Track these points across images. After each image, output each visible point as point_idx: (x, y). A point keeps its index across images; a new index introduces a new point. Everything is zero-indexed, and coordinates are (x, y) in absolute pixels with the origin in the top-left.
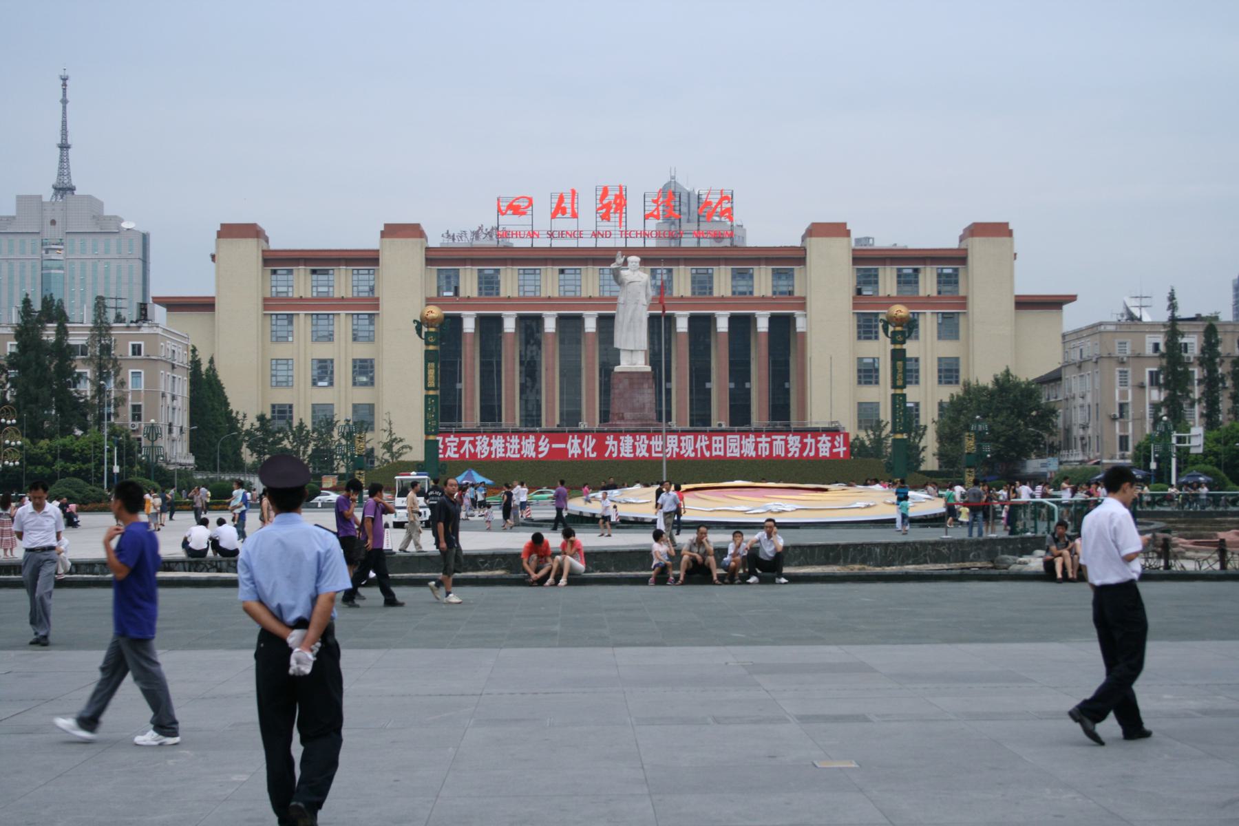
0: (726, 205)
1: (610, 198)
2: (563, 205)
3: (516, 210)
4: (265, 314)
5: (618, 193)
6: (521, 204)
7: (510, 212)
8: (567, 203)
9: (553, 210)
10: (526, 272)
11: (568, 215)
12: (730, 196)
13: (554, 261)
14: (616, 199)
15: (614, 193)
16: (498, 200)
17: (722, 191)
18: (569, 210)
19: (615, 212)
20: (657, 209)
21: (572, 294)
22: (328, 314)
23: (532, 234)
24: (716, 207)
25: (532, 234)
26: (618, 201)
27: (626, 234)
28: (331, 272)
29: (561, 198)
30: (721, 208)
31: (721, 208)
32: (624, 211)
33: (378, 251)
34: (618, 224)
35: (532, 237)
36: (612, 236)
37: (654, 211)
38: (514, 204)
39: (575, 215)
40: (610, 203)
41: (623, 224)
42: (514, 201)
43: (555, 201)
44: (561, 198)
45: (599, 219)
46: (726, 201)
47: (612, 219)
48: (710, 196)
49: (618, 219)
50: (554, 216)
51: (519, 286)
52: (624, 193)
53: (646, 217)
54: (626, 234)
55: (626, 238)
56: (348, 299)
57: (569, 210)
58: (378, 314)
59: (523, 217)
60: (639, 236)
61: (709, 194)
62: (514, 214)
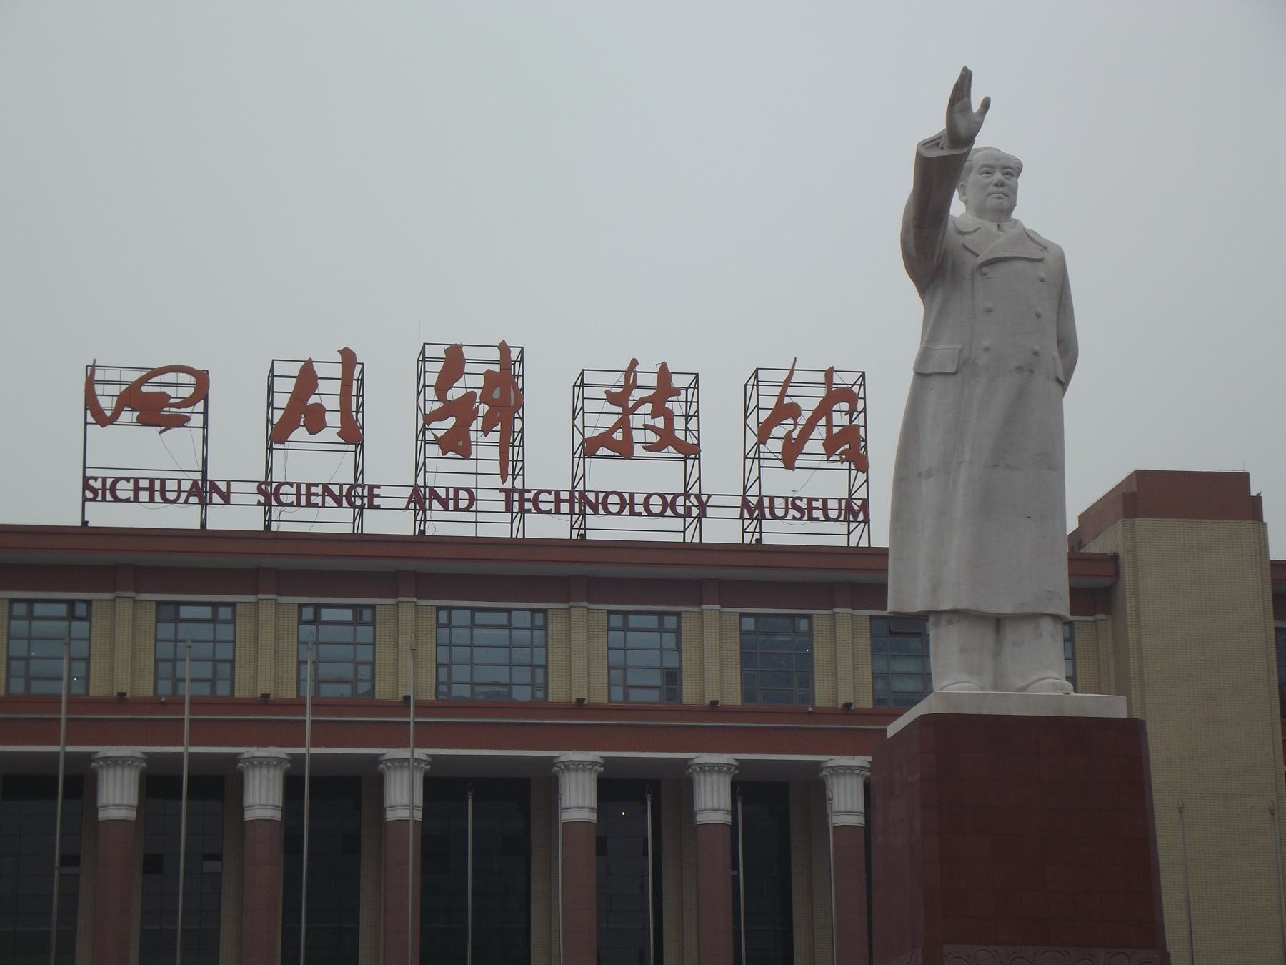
1: (472, 381)
2: (313, 400)
5: (496, 368)
6: (170, 391)
7: (128, 416)
8: (327, 395)
9: (278, 415)
10: (185, 612)
11: (330, 434)
14: (487, 391)
15: (483, 368)
17: (829, 373)
20: (624, 423)
21: (344, 690)
24: (811, 424)
25: (204, 490)
26: (497, 394)
27: (522, 501)
29: (307, 378)
30: (829, 425)
31: (829, 425)
34: (496, 467)
35: (204, 503)
36: (481, 506)
37: (613, 429)
38: (145, 389)
39: (352, 434)
40: (470, 397)
42: (144, 380)
43: (286, 386)
44: (307, 378)
45: (434, 450)
46: (845, 406)
48: (790, 391)
49: (495, 452)
50: (278, 434)
51: (157, 661)
57: (333, 419)
59: (174, 431)
61: (787, 383)
62: (142, 422)
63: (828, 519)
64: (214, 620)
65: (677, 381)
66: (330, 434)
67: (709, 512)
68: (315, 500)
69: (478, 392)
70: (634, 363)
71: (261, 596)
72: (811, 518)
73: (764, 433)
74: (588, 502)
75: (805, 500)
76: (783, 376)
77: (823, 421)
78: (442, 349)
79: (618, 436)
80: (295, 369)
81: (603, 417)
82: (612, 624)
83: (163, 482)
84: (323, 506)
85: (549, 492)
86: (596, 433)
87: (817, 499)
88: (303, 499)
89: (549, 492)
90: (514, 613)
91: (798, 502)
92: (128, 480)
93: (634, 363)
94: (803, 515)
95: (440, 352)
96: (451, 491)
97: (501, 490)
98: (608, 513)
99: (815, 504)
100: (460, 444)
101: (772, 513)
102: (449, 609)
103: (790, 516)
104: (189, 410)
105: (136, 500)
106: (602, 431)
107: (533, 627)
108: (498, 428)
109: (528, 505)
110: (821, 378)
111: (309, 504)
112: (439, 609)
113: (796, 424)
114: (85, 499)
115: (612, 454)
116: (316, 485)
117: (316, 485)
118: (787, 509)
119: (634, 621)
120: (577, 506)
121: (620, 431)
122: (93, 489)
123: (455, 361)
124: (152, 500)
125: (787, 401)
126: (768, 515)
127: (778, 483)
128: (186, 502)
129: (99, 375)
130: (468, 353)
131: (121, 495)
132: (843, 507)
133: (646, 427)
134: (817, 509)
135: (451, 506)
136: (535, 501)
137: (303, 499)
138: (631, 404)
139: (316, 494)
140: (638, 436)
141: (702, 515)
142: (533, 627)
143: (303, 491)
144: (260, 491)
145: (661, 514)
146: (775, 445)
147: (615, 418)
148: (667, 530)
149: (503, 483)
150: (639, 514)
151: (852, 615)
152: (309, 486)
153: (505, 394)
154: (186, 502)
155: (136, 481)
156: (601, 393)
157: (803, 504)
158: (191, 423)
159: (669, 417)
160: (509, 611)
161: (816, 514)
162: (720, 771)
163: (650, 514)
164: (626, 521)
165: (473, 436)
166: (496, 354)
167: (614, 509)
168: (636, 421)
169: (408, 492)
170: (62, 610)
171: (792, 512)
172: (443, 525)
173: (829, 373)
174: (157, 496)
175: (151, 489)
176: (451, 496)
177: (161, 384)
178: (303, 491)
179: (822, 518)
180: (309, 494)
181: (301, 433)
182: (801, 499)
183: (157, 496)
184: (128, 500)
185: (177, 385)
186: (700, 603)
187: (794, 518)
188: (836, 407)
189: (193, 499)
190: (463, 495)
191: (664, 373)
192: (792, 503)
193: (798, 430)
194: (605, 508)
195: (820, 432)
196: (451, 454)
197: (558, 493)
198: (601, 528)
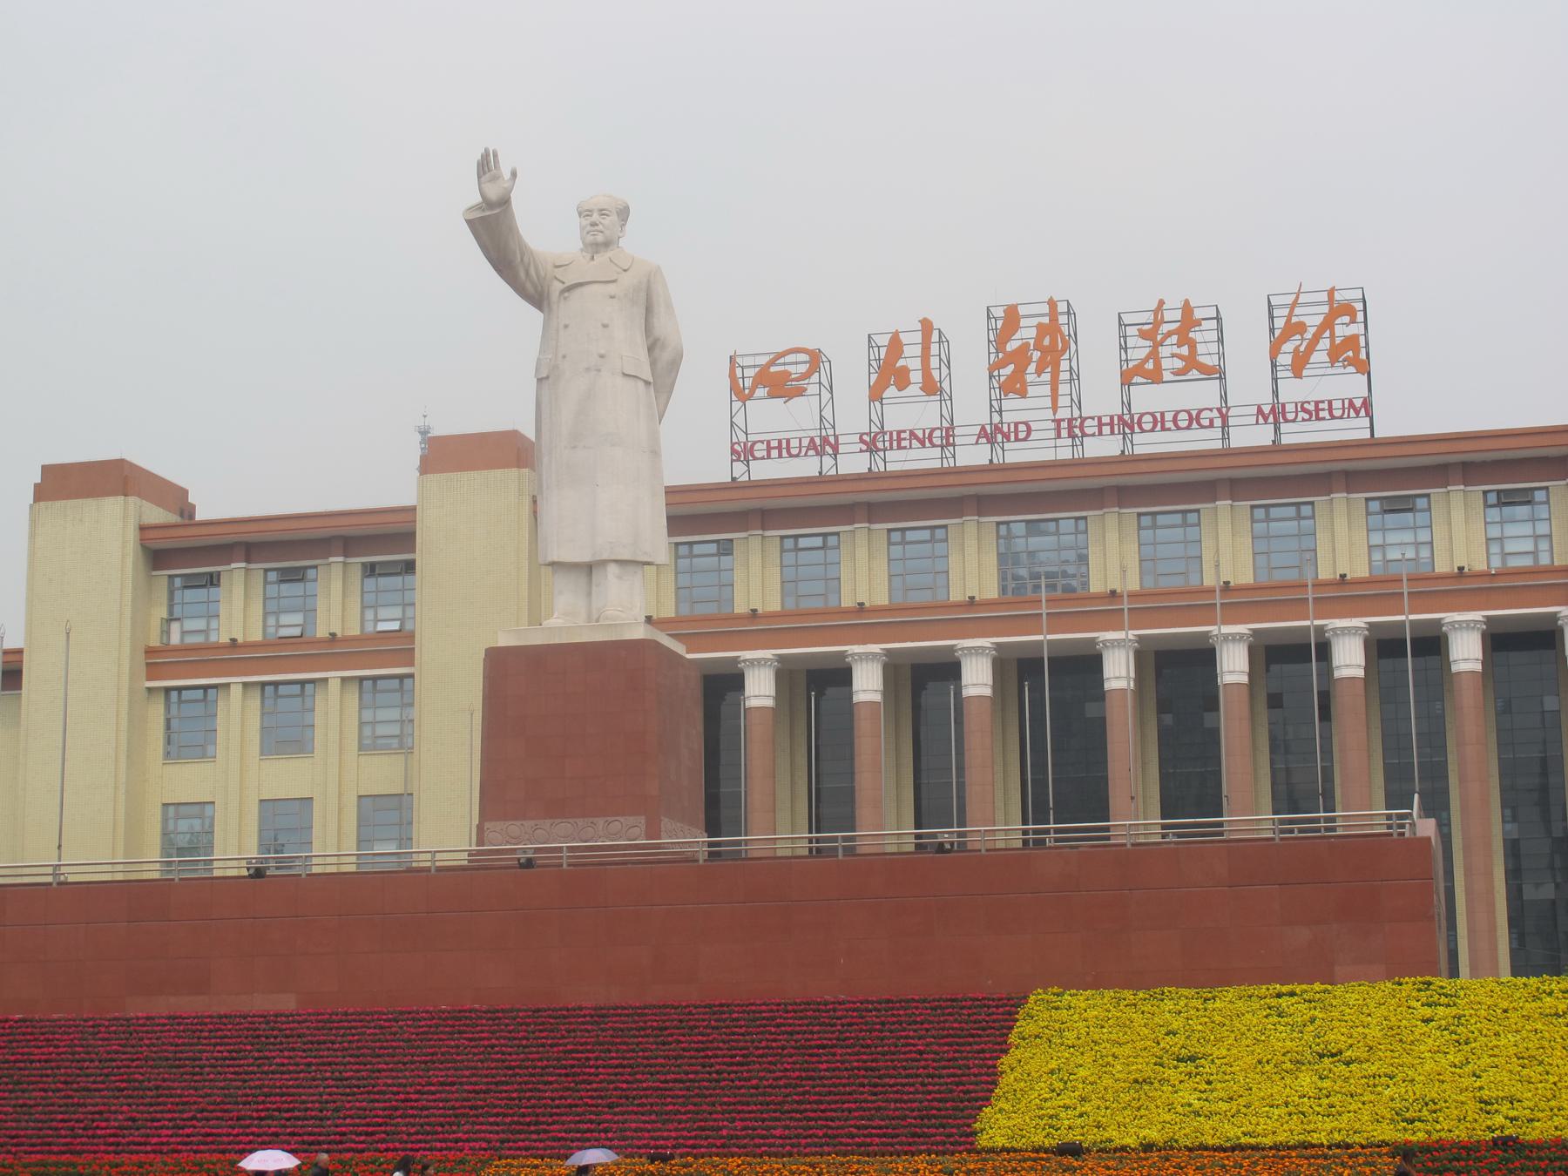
0: (1342, 330)
1: (1027, 333)
2: (901, 363)
3: (780, 386)
4: (149, 690)
5: (1046, 320)
6: (788, 368)
8: (911, 359)
9: (874, 377)
10: (803, 543)
11: (914, 389)
12: (1359, 306)
13: (873, 511)
15: (1035, 321)
16: (732, 359)
17: (1331, 292)
18: (916, 377)
19: (1039, 372)
20: (1154, 355)
22: (303, 683)
23: (825, 445)
26: (1046, 341)
27: (1070, 428)
28: (311, 573)
29: (896, 345)
30: (1332, 336)
31: (1332, 336)
32: (1064, 365)
33: (413, 509)
34: (1048, 402)
36: (1034, 435)
37: (1146, 360)
38: (773, 369)
39: (931, 387)
40: (1025, 347)
41: (1063, 401)
42: (772, 363)
44: (896, 345)
46: (1346, 319)
47: (1031, 391)
48: (1297, 311)
49: (1047, 390)
50: (876, 394)
52: (1063, 319)
53: (1126, 380)
54: (1074, 429)
55: (1072, 436)
56: (348, 640)
57: (916, 377)
58: (411, 676)
60: (1106, 430)
62: (771, 396)
63: (1333, 417)
64: (824, 547)
65: (1198, 314)
66: (914, 389)
67: (1231, 421)
68: (904, 443)
69: (1032, 342)
70: (1161, 303)
71: (856, 525)
72: (1318, 418)
73: (1275, 351)
74: (1125, 424)
75: (1313, 404)
76: (1290, 299)
77: (1327, 334)
78: (1002, 309)
79: (1150, 365)
80: (884, 340)
81: (1139, 350)
82: (1371, 510)
83: (788, 441)
84: (911, 447)
85: (1093, 418)
86: (1131, 364)
87: (1323, 402)
88: (895, 444)
89: (1093, 418)
90: (1011, 524)
91: (1306, 406)
92: (762, 442)
93: (1161, 303)
94: (1311, 416)
95: (999, 312)
96: (1012, 426)
97: (1053, 421)
98: (1143, 431)
99: (1321, 406)
100: (1018, 386)
101: (1284, 417)
102: (1007, 523)
103: (1299, 418)
104: (806, 382)
105: (769, 457)
106: (1136, 363)
107: (1077, 532)
108: (1049, 370)
109: (1077, 431)
110: (1324, 297)
111: (900, 447)
112: (998, 524)
113: (1302, 339)
114: (732, 461)
115: (1145, 381)
116: (904, 431)
117: (904, 431)
118: (1297, 412)
119: (1274, 512)
120: (1116, 428)
121: (1151, 361)
122: (744, 453)
123: (1012, 317)
124: (780, 456)
125: (1294, 320)
126: (1281, 420)
127: (1293, 391)
128: (806, 455)
129: (739, 360)
130: (1022, 310)
131: (757, 454)
132: (1346, 406)
133: (1173, 356)
134: (1323, 410)
135: (1012, 438)
136: (1081, 427)
137: (895, 444)
138: (1159, 337)
139: (905, 439)
140: (1166, 364)
141: (1225, 425)
142: (1077, 532)
143: (895, 437)
144: (862, 441)
145: (1188, 428)
146: (1285, 359)
147: (1148, 350)
148: (1205, 440)
149: (1054, 414)
150: (1169, 429)
151: (1464, 491)
152: (899, 433)
153: (1054, 341)
154: (806, 455)
155: (768, 442)
156: (1132, 331)
157: (1311, 407)
158: (808, 392)
159: (1192, 345)
160: (1056, 520)
161: (1322, 414)
162: (1468, 628)
163: (1179, 428)
164: (1159, 436)
165: (1029, 378)
166: (1045, 309)
167: (1147, 427)
168: (1164, 351)
169: (977, 430)
170: (713, 548)
171: (1301, 415)
172: (1016, 454)
173: (1331, 292)
174: (784, 451)
175: (779, 448)
176: (1012, 429)
177: (784, 364)
178: (895, 437)
179: (1328, 417)
180: (899, 440)
181: (891, 391)
182: (1309, 402)
183: (784, 451)
184: (763, 458)
185: (797, 363)
186: (1214, 500)
187: (1304, 420)
188: (1338, 321)
189: (811, 452)
190: (1022, 428)
191: (1187, 309)
192: (1302, 407)
193: (1305, 343)
194: (1140, 427)
195: (1324, 344)
196: (1011, 395)
197: (1100, 419)
198: (1147, 443)
